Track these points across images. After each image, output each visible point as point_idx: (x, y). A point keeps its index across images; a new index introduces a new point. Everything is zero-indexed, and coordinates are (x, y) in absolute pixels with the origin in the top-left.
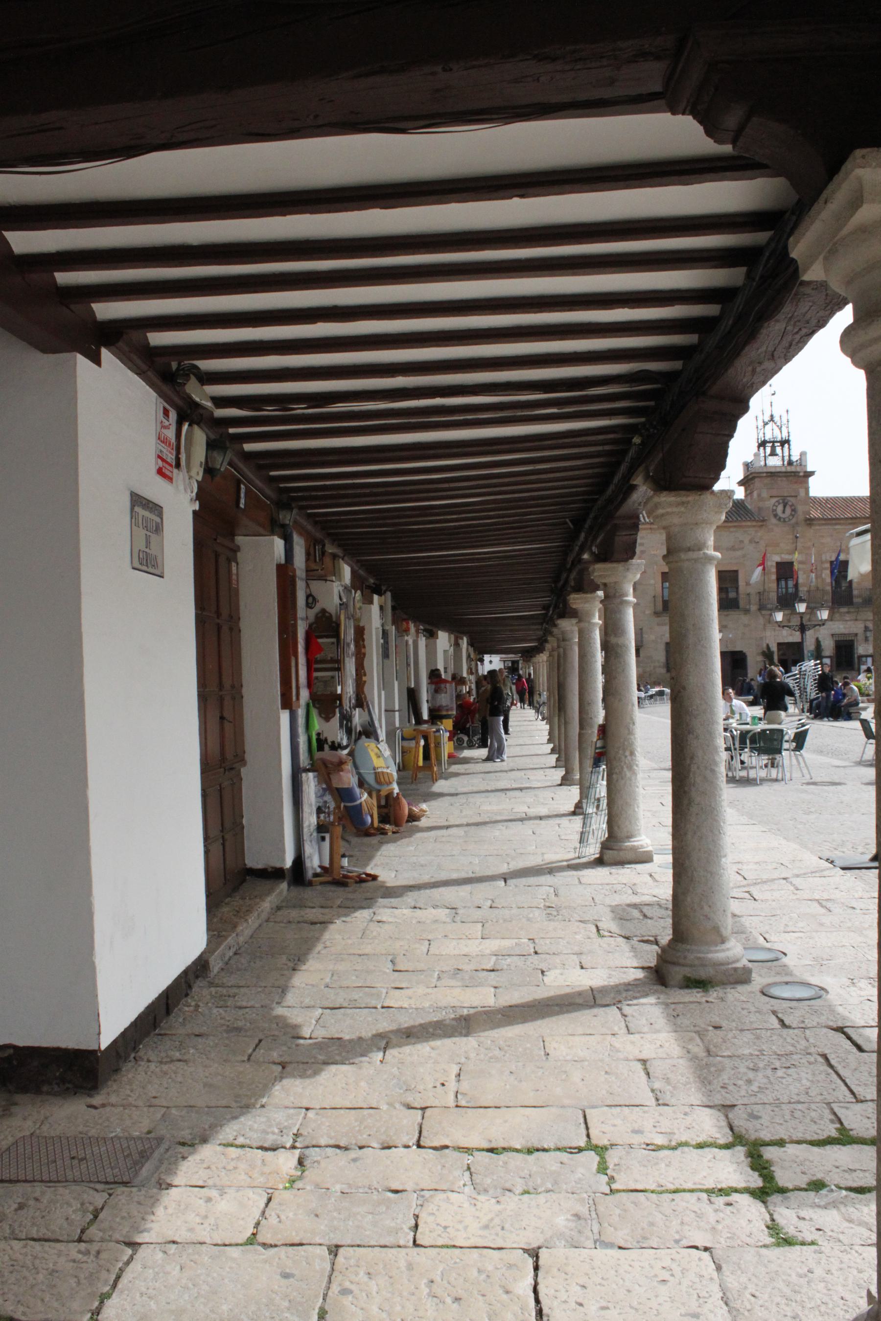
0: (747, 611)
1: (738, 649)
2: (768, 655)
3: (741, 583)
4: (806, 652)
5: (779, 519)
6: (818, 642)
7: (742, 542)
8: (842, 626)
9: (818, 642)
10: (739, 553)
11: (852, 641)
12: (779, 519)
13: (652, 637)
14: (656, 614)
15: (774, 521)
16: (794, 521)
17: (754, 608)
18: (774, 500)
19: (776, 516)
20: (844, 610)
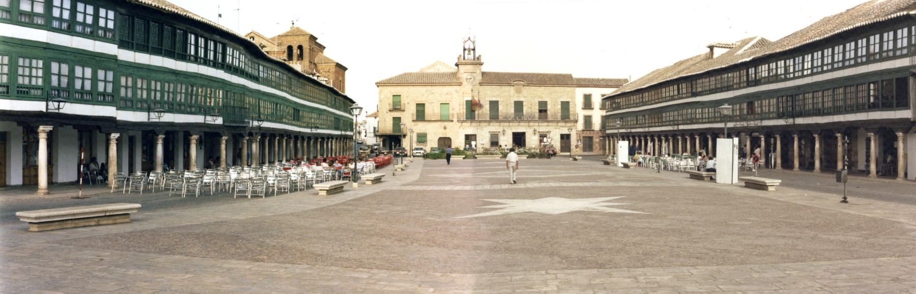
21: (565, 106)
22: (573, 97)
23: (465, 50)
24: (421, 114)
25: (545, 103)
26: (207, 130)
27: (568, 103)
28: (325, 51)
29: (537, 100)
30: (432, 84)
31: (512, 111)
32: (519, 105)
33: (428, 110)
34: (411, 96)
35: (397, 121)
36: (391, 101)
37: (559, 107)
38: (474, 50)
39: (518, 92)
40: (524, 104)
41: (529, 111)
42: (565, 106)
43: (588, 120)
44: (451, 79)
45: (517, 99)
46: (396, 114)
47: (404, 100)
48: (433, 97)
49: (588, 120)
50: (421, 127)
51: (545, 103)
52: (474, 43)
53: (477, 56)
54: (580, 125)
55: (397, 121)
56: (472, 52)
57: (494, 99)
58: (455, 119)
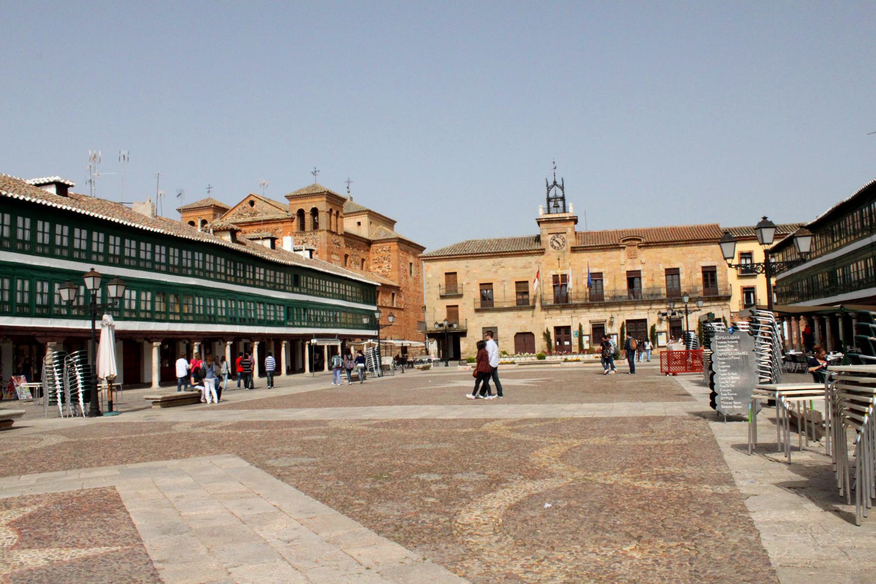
2: (547, 335)
10: (529, 270)
13: (474, 324)
14: (477, 311)
19: (552, 246)
21: (709, 274)
23: (549, 200)
24: (486, 303)
26: (165, 336)
28: (396, 226)
29: (662, 268)
30: (506, 256)
31: (624, 285)
32: (633, 278)
34: (471, 275)
35: (453, 311)
36: (442, 280)
37: (700, 275)
38: (563, 199)
39: (632, 257)
40: (643, 274)
41: (650, 285)
42: (709, 274)
43: (748, 292)
44: (532, 247)
45: (630, 268)
47: (461, 279)
48: (503, 276)
49: (748, 292)
50: (489, 319)
52: (562, 188)
54: (736, 302)
55: (453, 311)
56: (560, 203)
57: (595, 270)
58: (538, 304)
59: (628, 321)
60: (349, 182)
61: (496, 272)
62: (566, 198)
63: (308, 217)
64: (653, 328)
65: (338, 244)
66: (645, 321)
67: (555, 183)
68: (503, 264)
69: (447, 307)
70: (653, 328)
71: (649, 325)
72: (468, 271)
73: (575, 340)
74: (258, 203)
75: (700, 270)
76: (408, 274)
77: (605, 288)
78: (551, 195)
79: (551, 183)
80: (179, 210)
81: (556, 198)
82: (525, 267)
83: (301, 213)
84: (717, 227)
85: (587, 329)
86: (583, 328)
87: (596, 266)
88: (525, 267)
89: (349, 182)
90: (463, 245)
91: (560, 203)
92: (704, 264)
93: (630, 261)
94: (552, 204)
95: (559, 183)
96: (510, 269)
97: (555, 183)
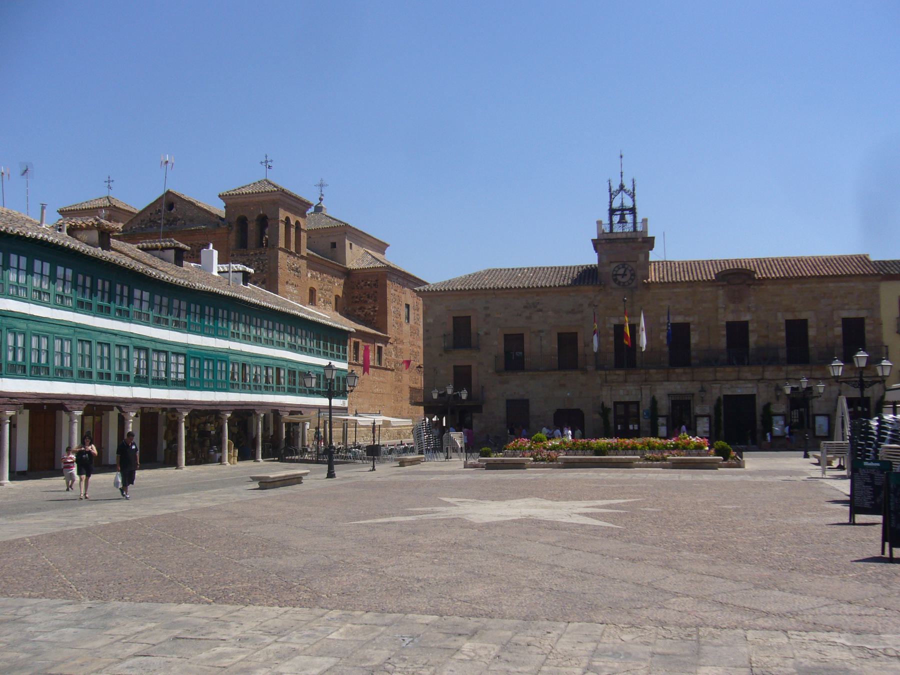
0: (584, 371)
1: (575, 407)
2: (604, 412)
3: (580, 344)
4: (641, 411)
5: (619, 283)
6: (654, 402)
7: (581, 305)
8: (679, 387)
9: (654, 402)
11: (689, 402)
12: (619, 283)
15: (614, 285)
16: (633, 284)
17: (590, 368)
18: (615, 265)
19: (615, 280)
20: (679, 370)
22: (874, 307)
23: (612, 212)
25: (802, 325)
27: (860, 322)
29: (781, 318)
31: (723, 343)
33: (531, 346)
37: (839, 331)
38: (633, 211)
40: (751, 327)
45: (731, 318)
46: (461, 358)
50: (517, 385)
51: (802, 325)
52: (633, 197)
53: (639, 219)
57: (679, 319)
59: (725, 396)
60: (321, 185)
61: (529, 318)
62: (637, 211)
63: (252, 227)
64: (767, 407)
65: (297, 270)
66: (752, 397)
67: (622, 187)
68: (539, 307)
69: (455, 367)
70: (767, 407)
71: (760, 403)
72: (488, 316)
73: (644, 421)
74: (178, 206)
75: (840, 323)
76: (403, 319)
77: (692, 346)
78: (616, 204)
79: (616, 187)
80: (61, 212)
81: (622, 209)
82: (572, 312)
83: (243, 222)
84: (863, 260)
85: (664, 405)
86: (659, 406)
87: (680, 314)
88: (572, 312)
89: (321, 185)
90: (478, 276)
91: (629, 218)
92: (845, 314)
93: (732, 306)
94: (616, 219)
95: (628, 186)
96: (550, 313)
97: (622, 187)
